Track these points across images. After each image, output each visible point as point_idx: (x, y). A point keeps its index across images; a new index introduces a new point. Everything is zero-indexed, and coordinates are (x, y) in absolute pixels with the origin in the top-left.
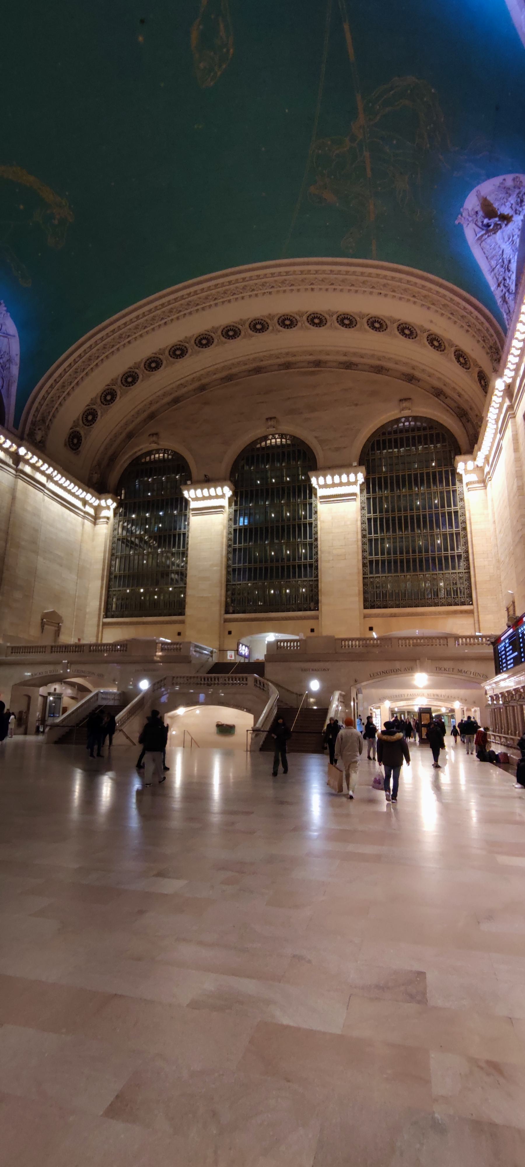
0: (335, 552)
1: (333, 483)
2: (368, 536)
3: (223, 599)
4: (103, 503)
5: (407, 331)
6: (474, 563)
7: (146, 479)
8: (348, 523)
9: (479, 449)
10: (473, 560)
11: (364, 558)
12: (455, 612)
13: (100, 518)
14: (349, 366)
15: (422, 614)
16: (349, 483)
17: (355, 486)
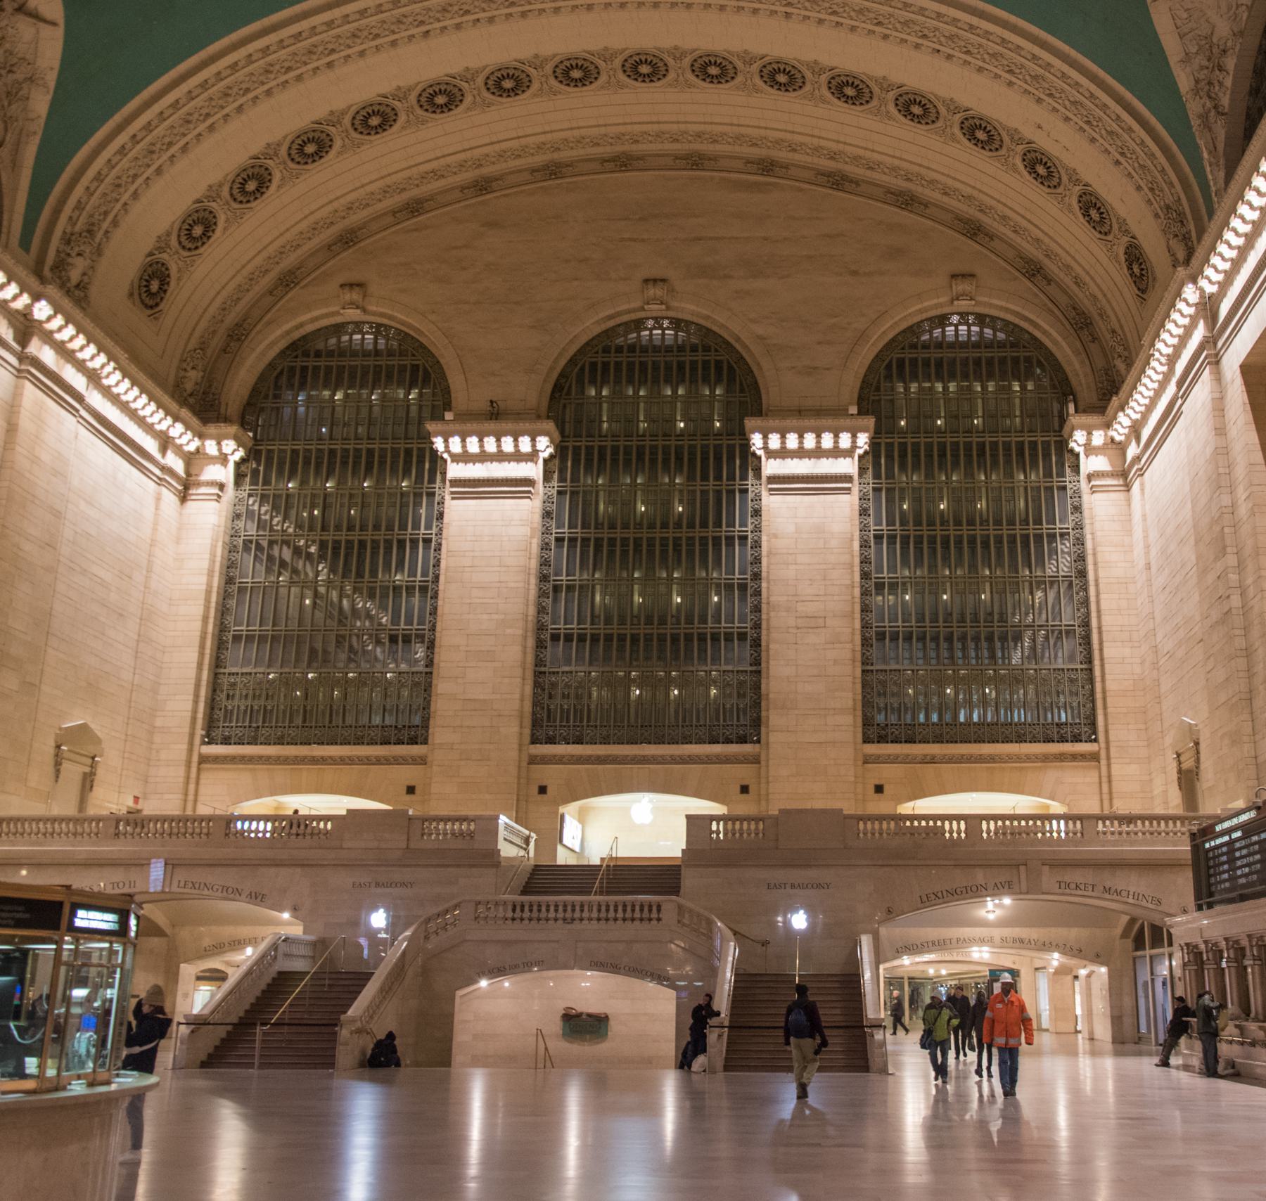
0: (801, 608)
1: (801, 447)
2: (874, 575)
3: (528, 707)
4: (211, 447)
5: (981, 133)
6: (1101, 650)
7: (326, 393)
8: (834, 543)
9: (1122, 408)
10: (1101, 643)
11: (865, 626)
12: (1061, 757)
13: (199, 484)
14: (838, 181)
15: (992, 759)
16: (836, 453)
17: (848, 460)
